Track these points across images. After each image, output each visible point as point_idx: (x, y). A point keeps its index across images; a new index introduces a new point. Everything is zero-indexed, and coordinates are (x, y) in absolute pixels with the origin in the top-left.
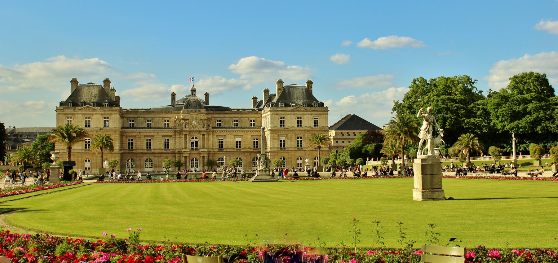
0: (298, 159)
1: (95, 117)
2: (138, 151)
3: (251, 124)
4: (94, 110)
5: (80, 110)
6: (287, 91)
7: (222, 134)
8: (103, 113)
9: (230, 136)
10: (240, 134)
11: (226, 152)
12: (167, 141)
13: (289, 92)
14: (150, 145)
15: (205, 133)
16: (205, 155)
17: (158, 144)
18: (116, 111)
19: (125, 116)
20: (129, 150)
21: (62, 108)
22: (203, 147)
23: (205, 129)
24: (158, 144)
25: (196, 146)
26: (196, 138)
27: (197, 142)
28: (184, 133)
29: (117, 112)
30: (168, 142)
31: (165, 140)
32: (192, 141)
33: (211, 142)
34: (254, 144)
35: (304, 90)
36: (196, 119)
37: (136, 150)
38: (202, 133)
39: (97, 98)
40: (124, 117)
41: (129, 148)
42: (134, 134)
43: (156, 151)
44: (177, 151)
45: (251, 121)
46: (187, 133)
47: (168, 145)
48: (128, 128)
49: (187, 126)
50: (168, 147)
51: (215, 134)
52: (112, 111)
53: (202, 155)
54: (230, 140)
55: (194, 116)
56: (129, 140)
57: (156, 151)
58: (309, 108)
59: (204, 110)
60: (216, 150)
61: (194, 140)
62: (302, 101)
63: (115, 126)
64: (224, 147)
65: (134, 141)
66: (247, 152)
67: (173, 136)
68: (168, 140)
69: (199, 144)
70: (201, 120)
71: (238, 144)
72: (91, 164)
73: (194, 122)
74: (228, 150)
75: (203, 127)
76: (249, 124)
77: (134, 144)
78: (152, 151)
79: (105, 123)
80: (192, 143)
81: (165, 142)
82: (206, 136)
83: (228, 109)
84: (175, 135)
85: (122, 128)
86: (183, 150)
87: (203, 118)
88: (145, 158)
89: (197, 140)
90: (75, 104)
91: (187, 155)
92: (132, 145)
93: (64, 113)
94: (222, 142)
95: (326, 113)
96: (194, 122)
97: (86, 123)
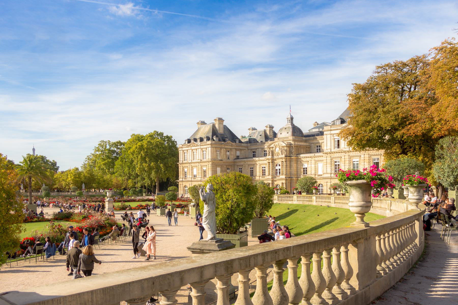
4: (197, 146)
8: (202, 147)
12: (264, 169)
15: (284, 160)
18: (208, 145)
19: (249, 148)
22: (283, 174)
23: (284, 156)
25: (280, 173)
26: (279, 165)
29: (209, 146)
40: (248, 149)
42: (242, 163)
46: (270, 161)
80: (277, 170)
81: (263, 170)
85: (235, 159)
96: (277, 149)
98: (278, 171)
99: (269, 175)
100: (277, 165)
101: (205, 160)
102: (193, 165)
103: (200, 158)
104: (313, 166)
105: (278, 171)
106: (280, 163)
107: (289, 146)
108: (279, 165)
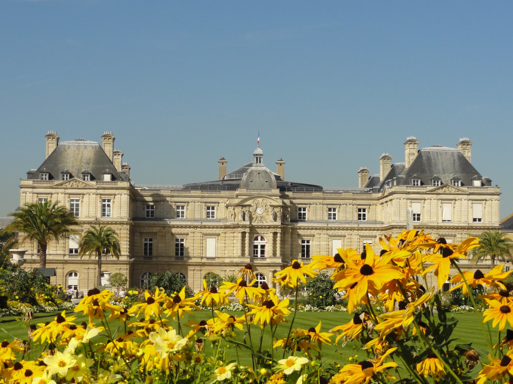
1: (86, 197)
2: (159, 259)
3: (360, 215)
5: (62, 184)
6: (424, 158)
8: (101, 192)
13: (429, 159)
15: (279, 231)
20: (145, 258)
21: (30, 182)
23: (278, 223)
25: (263, 252)
26: (262, 239)
27: (263, 247)
29: (125, 191)
32: (256, 243)
33: (288, 246)
35: (456, 156)
37: (157, 257)
39: (91, 165)
41: (146, 253)
42: (155, 230)
45: (360, 210)
46: (247, 230)
48: (144, 219)
49: (247, 218)
52: (117, 189)
53: (273, 269)
55: (260, 200)
56: (146, 240)
58: (465, 188)
59: (277, 191)
62: (452, 176)
65: (154, 242)
69: (266, 249)
70: (271, 206)
72: (79, 280)
75: (275, 219)
77: (154, 248)
79: (104, 210)
80: (256, 247)
82: (279, 235)
83: (318, 188)
87: (274, 203)
89: (263, 243)
90: (51, 177)
92: (151, 249)
93: (35, 190)
94: (308, 247)
95: (496, 197)
96: (259, 211)
98: (259, 249)
99: (243, 254)
100: (256, 239)
101: (105, 219)
103: (92, 214)
104: (323, 243)
105: (259, 249)
106: (269, 236)
107: (284, 207)
108: (262, 239)
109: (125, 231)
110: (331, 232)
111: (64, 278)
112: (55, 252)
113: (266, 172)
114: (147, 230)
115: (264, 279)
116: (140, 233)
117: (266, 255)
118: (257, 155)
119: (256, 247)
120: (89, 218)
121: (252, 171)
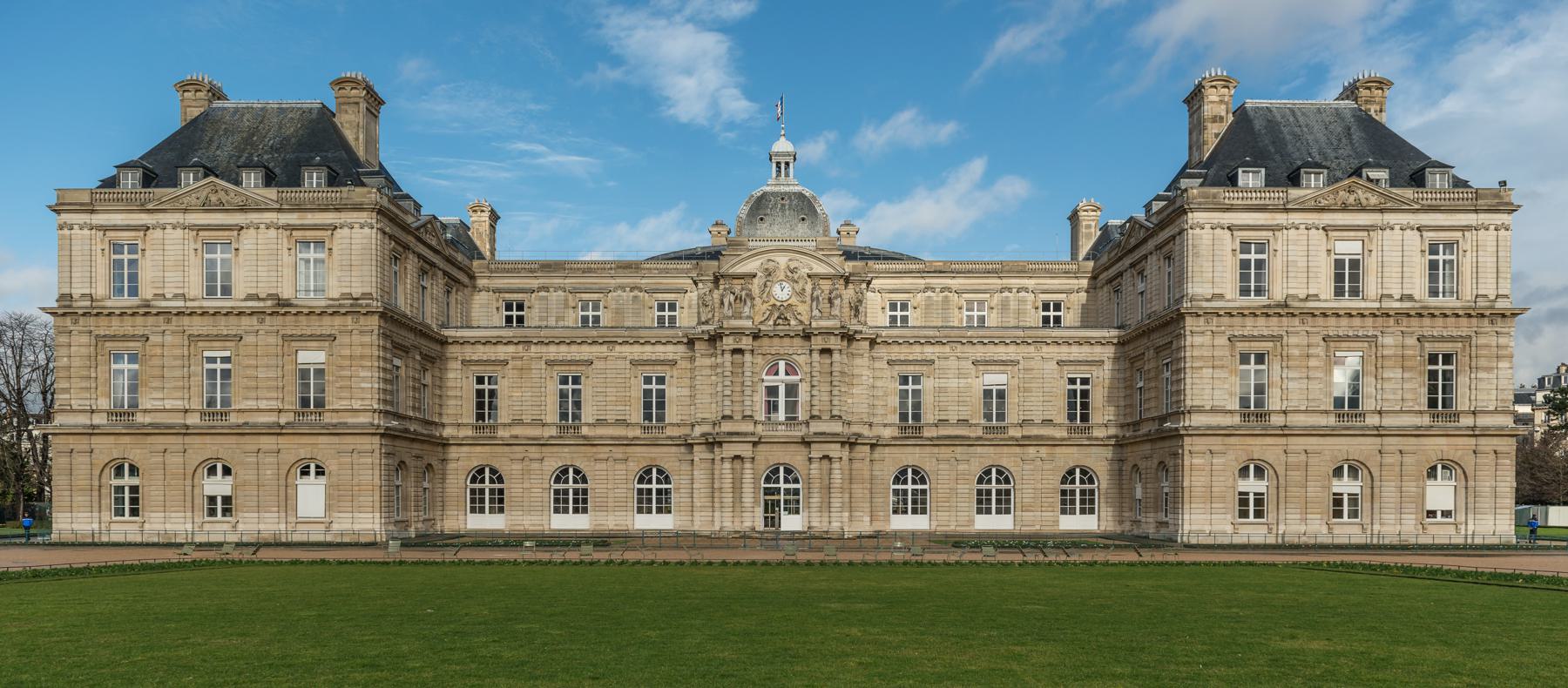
0: (1338, 472)
7: (917, 352)
9: (953, 363)
10: (1002, 352)
11: (937, 442)
12: (654, 387)
14: (577, 405)
16: (835, 450)
17: (611, 395)
24: (611, 395)
25: (792, 407)
27: (792, 390)
28: (729, 343)
30: (661, 394)
31: (648, 380)
32: (770, 380)
34: (1072, 406)
36: (792, 275)
38: (818, 343)
43: (600, 431)
44: (698, 431)
47: (661, 405)
50: (661, 418)
51: (881, 351)
54: (953, 383)
55: (782, 260)
57: (600, 431)
60: (887, 433)
61: (781, 379)
63: (356, 292)
64: (928, 416)
66: (1039, 441)
67: (683, 364)
68: (661, 380)
71: (995, 399)
72: (235, 487)
73: (782, 292)
74: (944, 432)
76: (1034, 318)
78: (585, 431)
80: (772, 391)
81: (647, 393)
84: (692, 359)
86: (727, 427)
87: (820, 268)
88: (552, 465)
89: (792, 378)
91: (745, 450)
97: (211, 277)
102: (198, 326)
109: (367, 339)
110: (979, 352)
111: (189, 482)
112: (158, 404)
113: (801, 196)
114: (481, 352)
115: (796, 481)
116: (463, 362)
117: (802, 415)
118: (778, 154)
119: (772, 391)
120: (259, 299)
121: (764, 195)
